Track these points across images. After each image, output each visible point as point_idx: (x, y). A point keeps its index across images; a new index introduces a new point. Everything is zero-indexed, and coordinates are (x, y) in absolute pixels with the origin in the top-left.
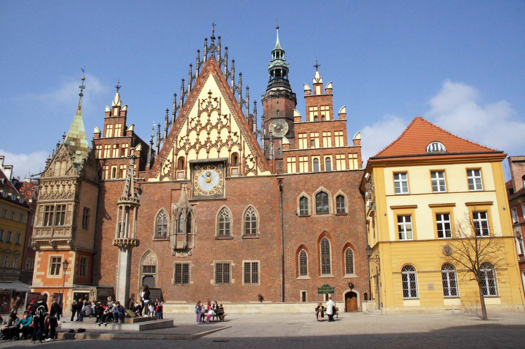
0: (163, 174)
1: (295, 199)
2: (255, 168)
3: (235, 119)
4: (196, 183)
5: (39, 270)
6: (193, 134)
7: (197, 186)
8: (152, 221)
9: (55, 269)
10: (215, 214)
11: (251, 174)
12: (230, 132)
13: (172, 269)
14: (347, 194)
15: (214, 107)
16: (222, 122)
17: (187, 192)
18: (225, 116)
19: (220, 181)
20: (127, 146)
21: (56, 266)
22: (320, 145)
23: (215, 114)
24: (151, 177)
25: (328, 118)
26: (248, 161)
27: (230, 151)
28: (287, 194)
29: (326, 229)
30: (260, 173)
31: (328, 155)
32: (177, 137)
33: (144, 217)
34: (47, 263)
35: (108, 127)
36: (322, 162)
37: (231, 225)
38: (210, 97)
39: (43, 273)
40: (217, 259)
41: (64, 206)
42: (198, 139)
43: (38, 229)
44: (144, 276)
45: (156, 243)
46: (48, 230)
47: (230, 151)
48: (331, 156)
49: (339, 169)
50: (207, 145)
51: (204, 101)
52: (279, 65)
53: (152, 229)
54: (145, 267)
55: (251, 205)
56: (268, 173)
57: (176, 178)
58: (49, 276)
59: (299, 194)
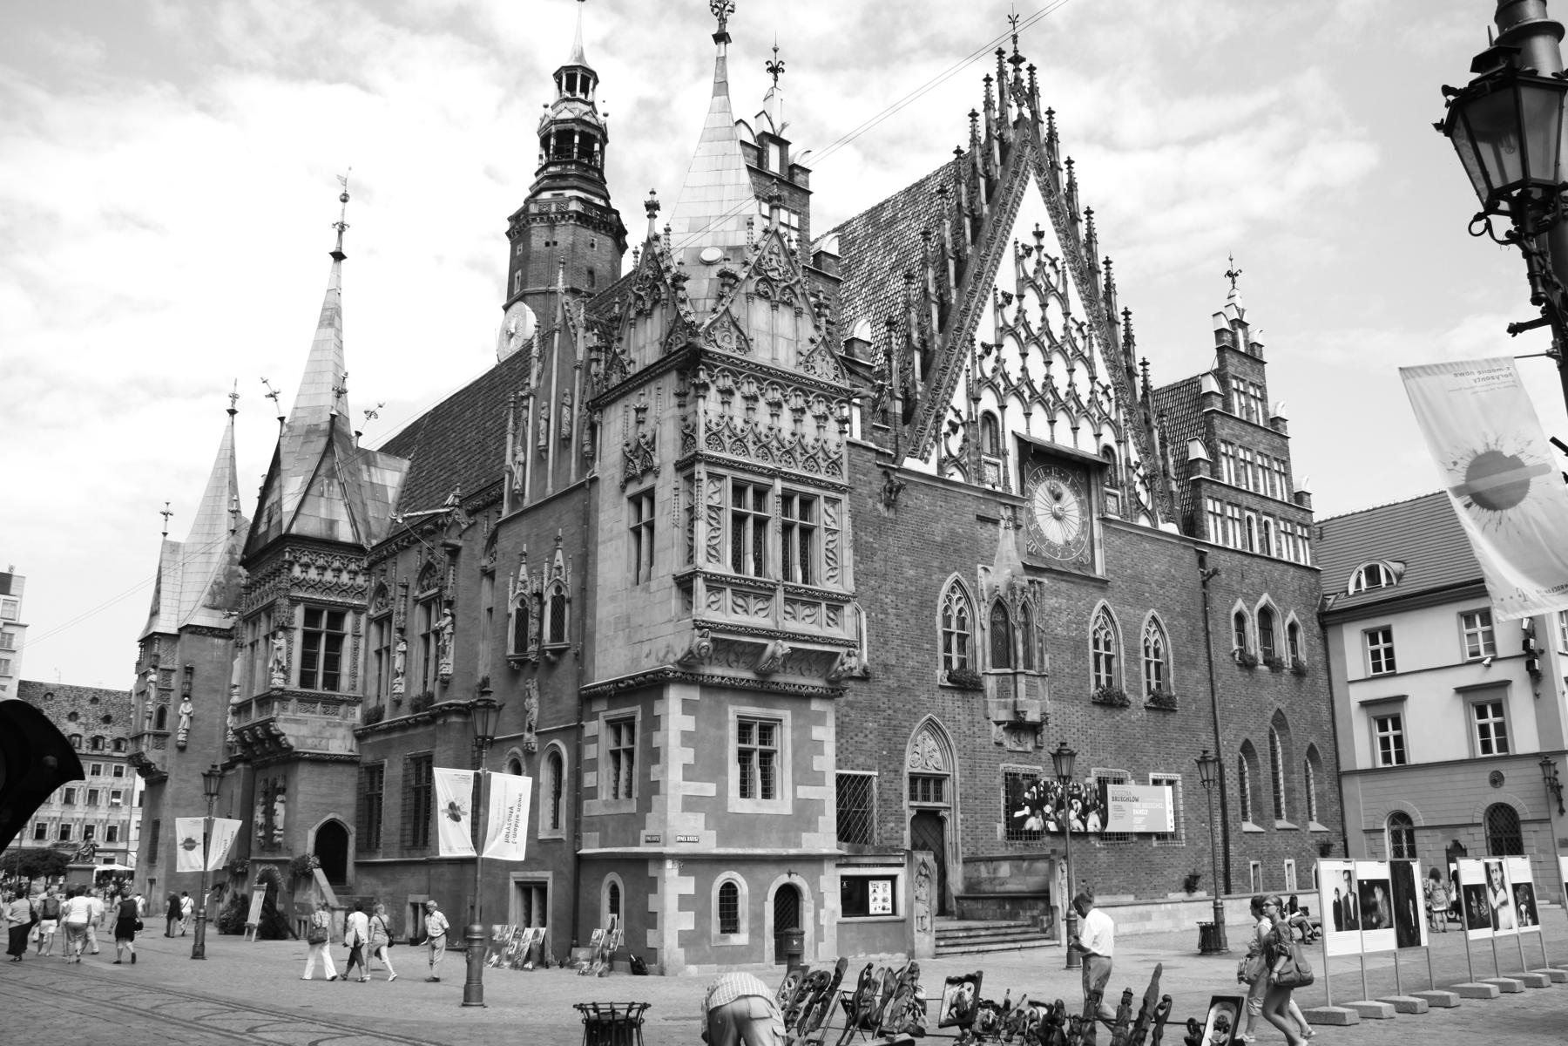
1: (1228, 615)
5: (689, 773)
6: (1010, 345)
8: (933, 615)
9: (758, 772)
10: (1087, 623)
11: (1143, 521)
12: (1093, 379)
13: (994, 790)
14: (1304, 622)
15: (1053, 279)
17: (1012, 532)
18: (1080, 329)
19: (1084, 523)
21: (756, 757)
22: (1256, 485)
23: (1054, 305)
24: (912, 455)
26: (1136, 478)
27: (1098, 436)
28: (1217, 601)
29: (1282, 706)
30: (1163, 527)
33: (907, 596)
34: (722, 743)
37: (1120, 663)
38: (1040, 248)
39: (710, 789)
40: (1099, 764)
41: (807, 503)
42: (1024, 369)
43: (716, 584)
44: (914, 813)
45: (948, 696)
46: (764, 592)
47: (1098, 436)
52: (593, 121)
53: (934, 642)
54: (914, 778)
56: (1172, 528)
57: (981, 480)
58: (737, 805)
59: (1234, 603)
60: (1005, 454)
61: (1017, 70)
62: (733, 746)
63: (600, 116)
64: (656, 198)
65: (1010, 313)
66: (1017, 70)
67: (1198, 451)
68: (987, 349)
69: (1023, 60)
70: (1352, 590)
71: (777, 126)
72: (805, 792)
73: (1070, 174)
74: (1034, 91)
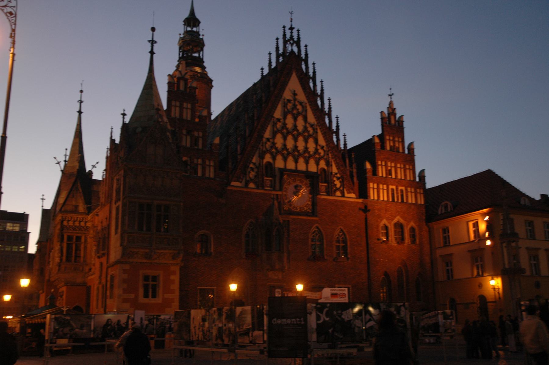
0: (248, 179)
2: (341, 189)
3: (321, 131)
4: (286, 195)
7: (286, 199)
9: (150, 291)
15: (300, 110)
16: (309, 131)
18: (312, 126)
20: (201, 134)
22: (396, 176)
25: (401, 150)
26: (335, 179)
31: (402, 186)
32: (262, 137)
35: (173, 103)
36: (397, 193)
38: (295, 100)
39: (132, 296)
48: (403, 188)
49: (410, 201)
50: (296, 154)
51: (289, 101)
55: (342, 228)
58: (142, 300)
59: (381, 220)
60: (273, 176)
61: (292, 33)
62: (141, 283)
63: (201, 37)
64: (126, 112)
65: (279, 125)
66: (292, 33)
67: (368, 166)
68: (268, 140)
69: (294, 28)
70: (439, 213)
71: (183, 73)
72: (167, 296)
73: (314, 68)
74: (299, 38)
